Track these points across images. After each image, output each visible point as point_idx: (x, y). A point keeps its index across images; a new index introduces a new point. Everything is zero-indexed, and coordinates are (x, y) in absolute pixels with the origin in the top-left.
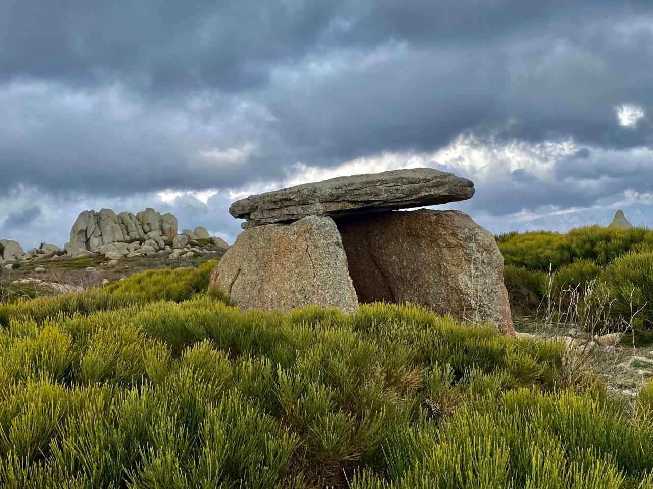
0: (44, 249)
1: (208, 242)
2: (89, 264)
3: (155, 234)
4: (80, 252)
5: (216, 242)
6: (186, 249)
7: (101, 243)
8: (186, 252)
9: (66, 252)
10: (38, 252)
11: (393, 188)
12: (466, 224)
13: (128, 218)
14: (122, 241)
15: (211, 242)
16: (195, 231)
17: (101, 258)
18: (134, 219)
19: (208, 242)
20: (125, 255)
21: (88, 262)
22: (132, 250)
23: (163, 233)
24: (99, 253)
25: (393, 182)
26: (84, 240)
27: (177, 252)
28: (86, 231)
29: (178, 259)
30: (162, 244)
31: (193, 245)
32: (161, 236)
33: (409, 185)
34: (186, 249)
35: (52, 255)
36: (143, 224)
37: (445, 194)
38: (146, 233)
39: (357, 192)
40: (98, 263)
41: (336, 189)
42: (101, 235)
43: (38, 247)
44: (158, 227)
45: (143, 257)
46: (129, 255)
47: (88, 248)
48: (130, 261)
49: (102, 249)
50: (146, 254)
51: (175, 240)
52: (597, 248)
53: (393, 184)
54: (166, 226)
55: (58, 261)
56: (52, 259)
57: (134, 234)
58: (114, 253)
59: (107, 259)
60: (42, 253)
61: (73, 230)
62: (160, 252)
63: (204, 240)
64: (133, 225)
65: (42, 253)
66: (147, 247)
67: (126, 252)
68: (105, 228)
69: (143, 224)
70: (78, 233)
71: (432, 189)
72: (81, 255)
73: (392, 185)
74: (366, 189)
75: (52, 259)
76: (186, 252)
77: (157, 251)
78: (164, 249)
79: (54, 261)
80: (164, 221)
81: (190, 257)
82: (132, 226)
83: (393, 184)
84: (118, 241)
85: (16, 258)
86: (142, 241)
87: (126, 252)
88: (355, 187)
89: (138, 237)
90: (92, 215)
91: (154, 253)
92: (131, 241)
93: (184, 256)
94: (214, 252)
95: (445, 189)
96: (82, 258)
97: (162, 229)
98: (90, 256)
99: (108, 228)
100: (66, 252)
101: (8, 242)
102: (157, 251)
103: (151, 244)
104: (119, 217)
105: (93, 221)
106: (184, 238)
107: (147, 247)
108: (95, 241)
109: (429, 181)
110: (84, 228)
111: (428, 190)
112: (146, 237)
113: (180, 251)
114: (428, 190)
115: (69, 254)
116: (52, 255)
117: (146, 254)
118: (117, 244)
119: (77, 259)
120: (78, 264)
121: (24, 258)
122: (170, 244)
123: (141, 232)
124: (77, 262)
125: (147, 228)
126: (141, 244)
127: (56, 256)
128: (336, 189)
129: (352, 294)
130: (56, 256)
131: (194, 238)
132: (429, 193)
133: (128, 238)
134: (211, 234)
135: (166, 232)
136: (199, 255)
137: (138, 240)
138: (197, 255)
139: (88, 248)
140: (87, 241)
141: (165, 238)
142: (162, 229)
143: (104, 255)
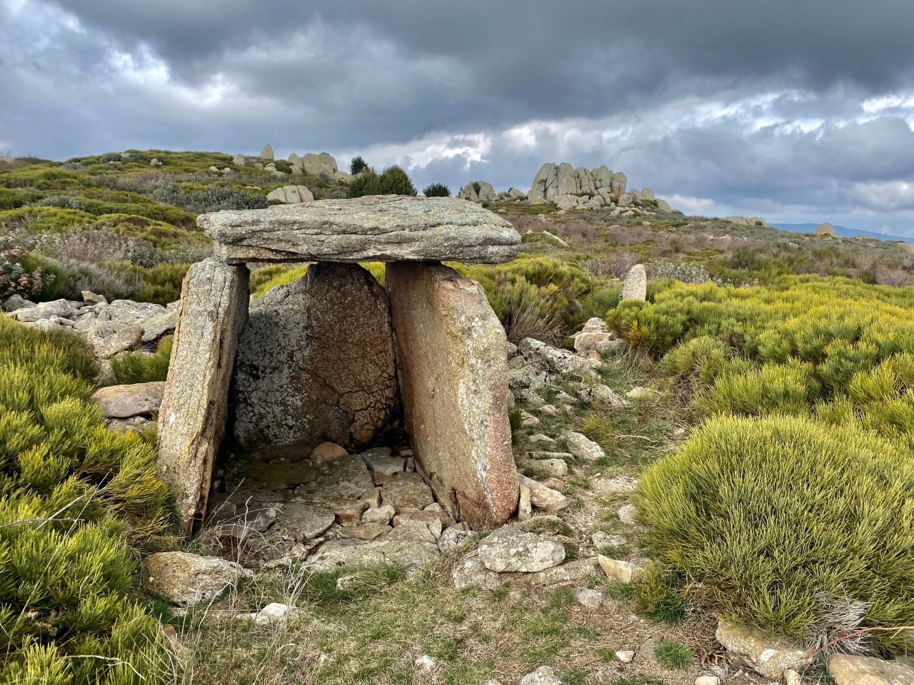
0: (511, 193)
1: (652, 204)
2: (541, 211)
3: (604, 191)
4: (537, 199)
5: (659, 204)
6: (627, 208)
7: (556, 193)
8: (627, 211)
9: (527, 198)
10: (506, 195)
11: (315, 237)
12: (465, 307)
13: (583, 172)
14: (574, 194)
15: (655, 204)
16: (642, 191)
17: (554, 207)
18: (588, 174)
19: (652, 204)
20: (574, 207)
21: (542, 209)
22: (580, 203)
23: (612, 191)
24: (553, 202)
25: (315, 228)
26: (543, 189)
27: (618, 209)
28: (546, 182)
29: (618, 217)
30: (608, 200)
31: (637, 205)
32: (609, 193)
33: (340, 237)
34: (627, 208)
35: (515, 200)
36: (595, 181)
37: (411, 257)
38: (596, 189)
39: (265, 235)
40: (550, 212)
41: (232, 226)
42: (557, 187)
43: (507, 191)
44: (608, 184)
45: (589, 210)
46: (578, 208)
47: (545, 197)
48: (575, 213)
49: (556, 199)
50: (592, 208)
51: (621, 199)
52: (829, 349)
53: (316, 230)
54: (616, 184)
55: (519, 205)
56: (515, 203)
57: (586, 189)
58: (565, 203)
59: (558, 209)
60: (509, 196)
61: (536, 179)
62: (605, 207)
63: (649, 201)
64: (587, 180)
65: (509, 196)
66: (595, 202)
67: (576, 204)
68: (561, 180)
69: (595, 181)
70: (539, 183)
71: (389, 247)
72: (537, 203)
73: (311, 231)
74: (278, 232)
75: (515, 203)
76: (627, 211)
77: (602, 206)
78: (609, 206)
79: (515, 205)
80: (615, 179)
81: (630, 217)
82: (585, 182)
83: (316, 230)
84: (571, 194)
85: (488, 198)
86: (591, 196)
87: (575, 204)
88: (262, 227)
89: (589, 192)
90: (553, 167)
91: (599, 208)
92: (582, 195)
93: (625, 214)
94: (654, 214)
95: (412, 249)
96: (537, 205)
97: (611, 186)
98: (545, 205)
99: (565, 180)
100: (527, 198)
101: (484, 184)
102: (602, 206)
103: (598, 200)
104: (576, 171)
105: (553, 172)
106: (629, 198)
107: (595, 202)
108: (551, 192)
109: (384, 232)
110: (545, 178)
111: (380, 247)
112: (596, 192)
113: (622, 209)
114: (380, 247)
115: (529, 200)
116: (515, 200)
117: (592, 208)
118: (569, 196)
119: (534, 206)
120: (532, 210)
121: (494, 199)
122: (616, 202)
123: (593, 187)
124: (533, 208)
125: (598, 184)
126: (590, 199)
127: (518, 201)
128: (232, 226)
129: (201, 398)
130: (518, 201)
131: (639, 199)
132: (384, 252)
133: (580, 192)
134: (657, 197)
135: (615, 190)
136: (639, 215)
137: (588, 194)
138: (636, 214)
139: (545, 197)
140: (546, 190)
141: (613, 195)
142: (611, 186)
143: (556, 204)
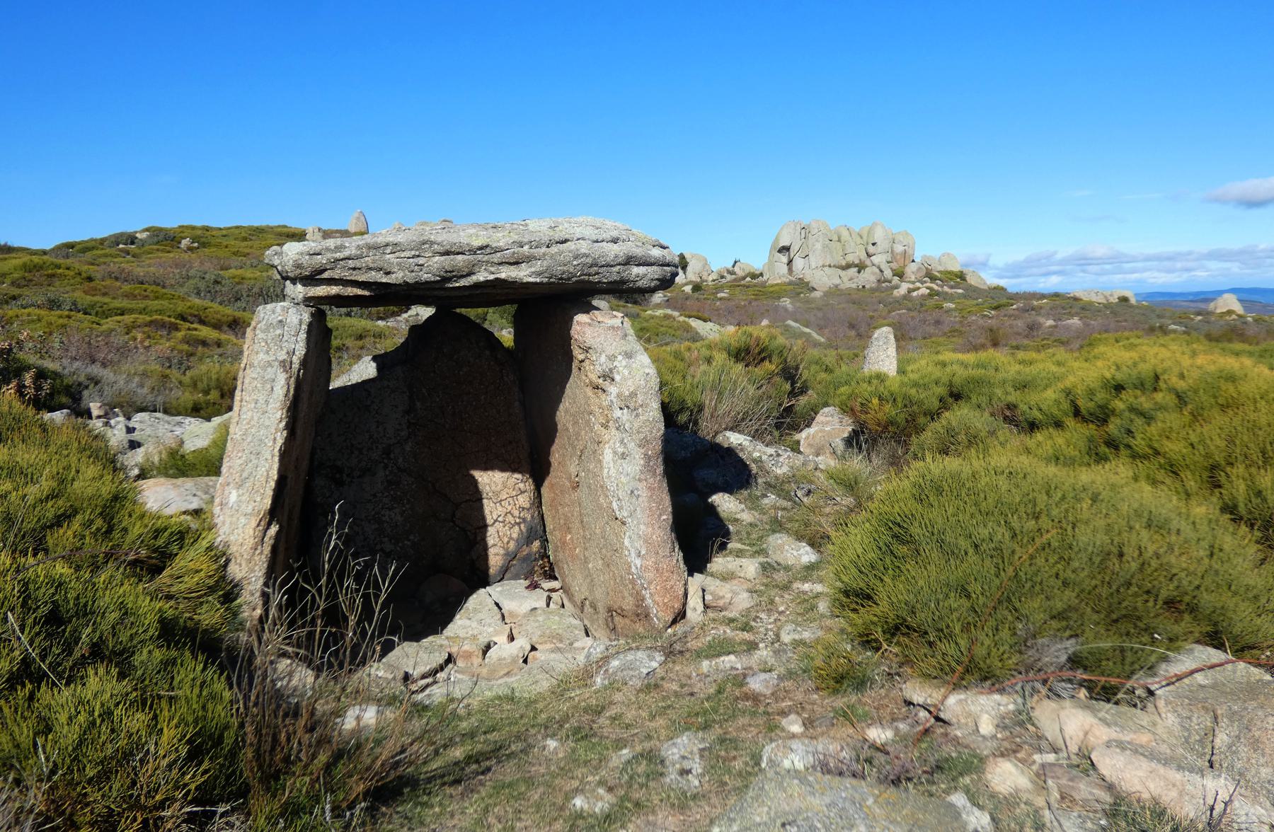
0: (736, 269)
5: (968, 278)
6: (918, 284)
8: (919, 288)
11: (411, 260)
14: (834, 266)
19: (957, 276)
21: (785, 290)
34: (918, 284)
35: (744, 278)
37: (531, 280)
39: (351, 263)
43: (729, 266)
47: (790, 270)
50: (864, 287)
52: (1119, 405)
53: (413, 253)
55: (748, 287)
56: (743, 282)
63: (950, 273)
73: (407, 254)
74: (367, 259)
75: (743, 282)
76: (919, 288)
78: (890, 282)
79: (744, 286)
84: (830, 266)
86: (861, 267)
88: (346, 253)
89: (857, 262)
92: (848, 266)
93: (915, 294)
94: (960, 291)
95: (533, 270)
96: (777, 285)
98: (790, 283)
100: (761, 275)
103: (874, 273)
108: (799, 263)
111: (492, 269)
112: (868, 262)
113: (911, 286)
114: (492, 269)
116: (744, 278)
118: (826, 269)
119: (772, 286)
121: (710, 278)
122: (900, 275)
124: (771, 289)
126: (859, 272)
127: (748, 279)
130: (748, 279)
131: (937, 268)
132: (498, 276)
137: (856, 266)
139: (790, 270)
140: (790, 262)
141: (894, 265)
